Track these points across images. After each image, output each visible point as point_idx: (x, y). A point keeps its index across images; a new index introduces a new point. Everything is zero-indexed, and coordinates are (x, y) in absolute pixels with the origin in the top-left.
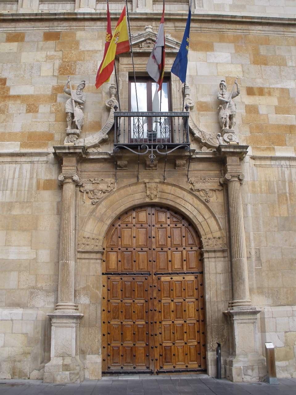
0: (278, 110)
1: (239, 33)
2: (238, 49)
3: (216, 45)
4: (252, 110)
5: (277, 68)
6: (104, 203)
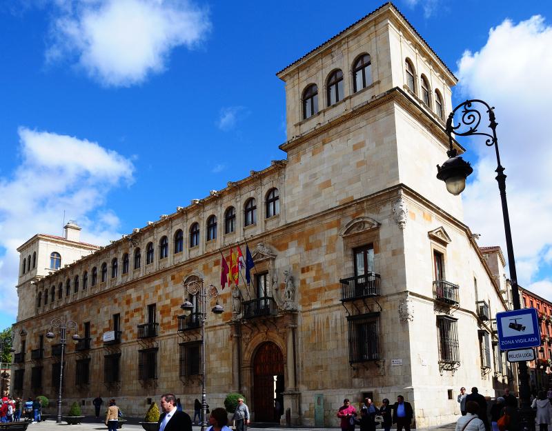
0: (316, 279)
1: (300, 231)
2: (299, 244)
3: (290, 243)
4: (303, 282)
5: (316, 250)
6: (250, 344)
